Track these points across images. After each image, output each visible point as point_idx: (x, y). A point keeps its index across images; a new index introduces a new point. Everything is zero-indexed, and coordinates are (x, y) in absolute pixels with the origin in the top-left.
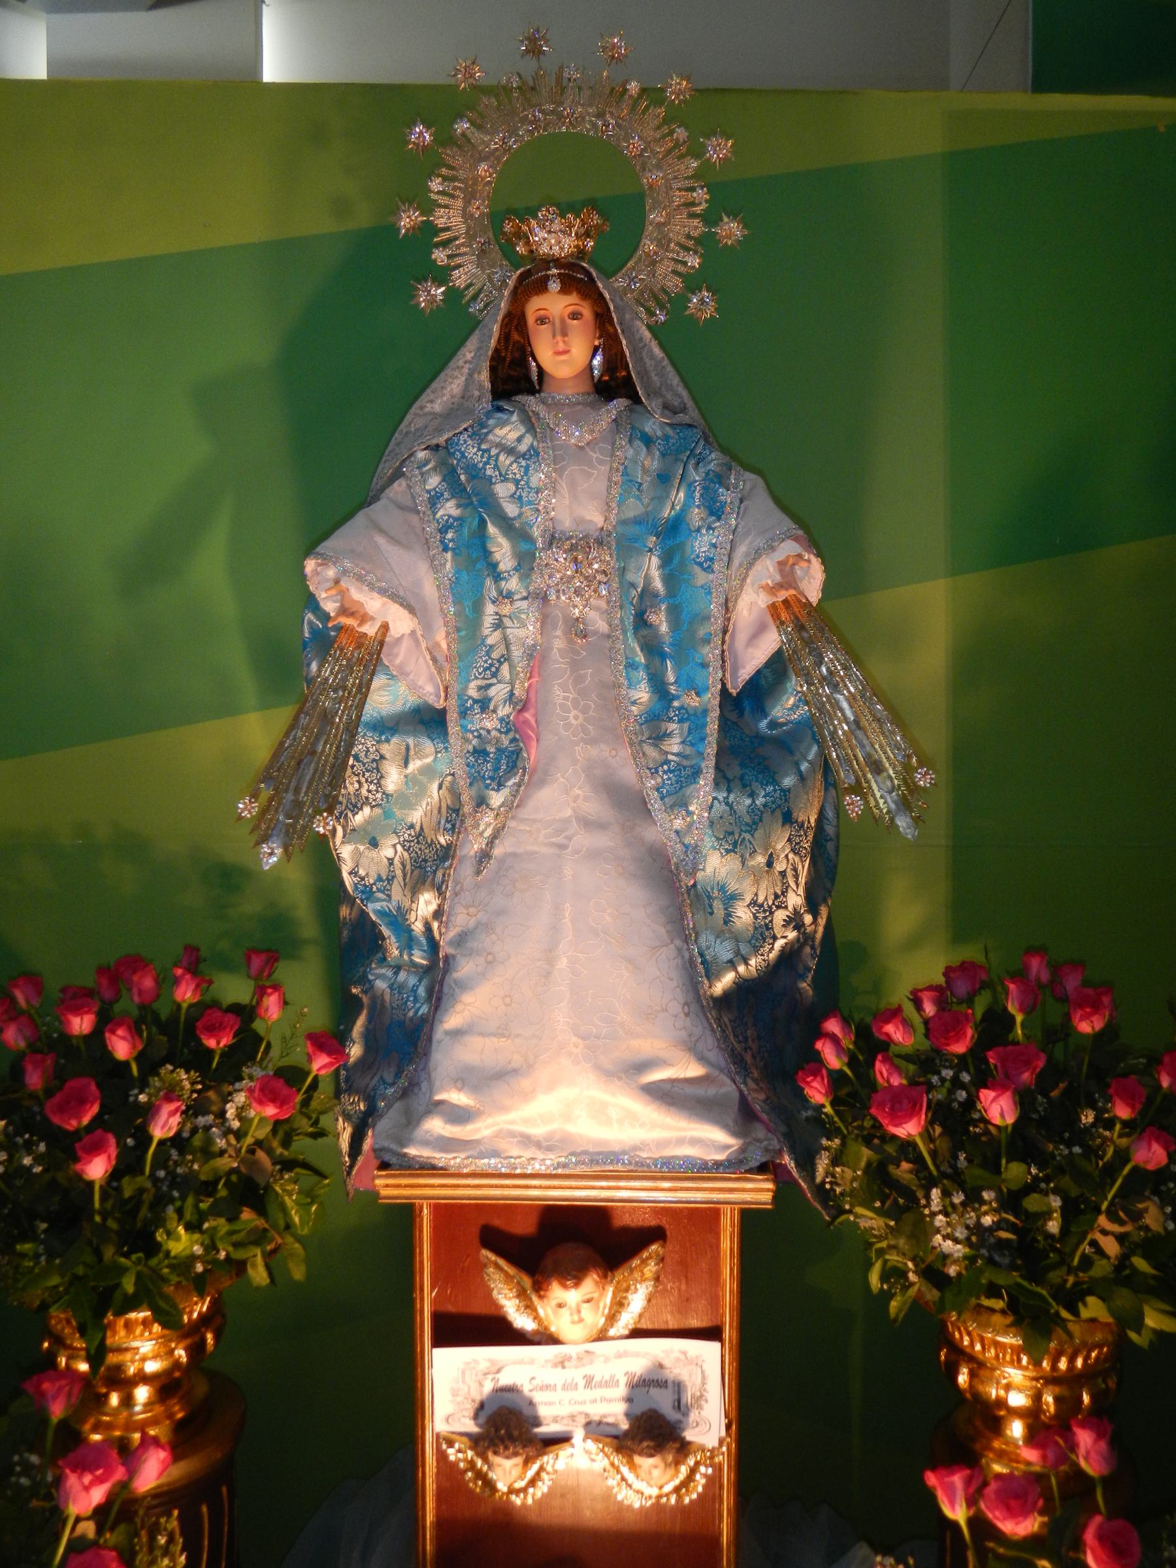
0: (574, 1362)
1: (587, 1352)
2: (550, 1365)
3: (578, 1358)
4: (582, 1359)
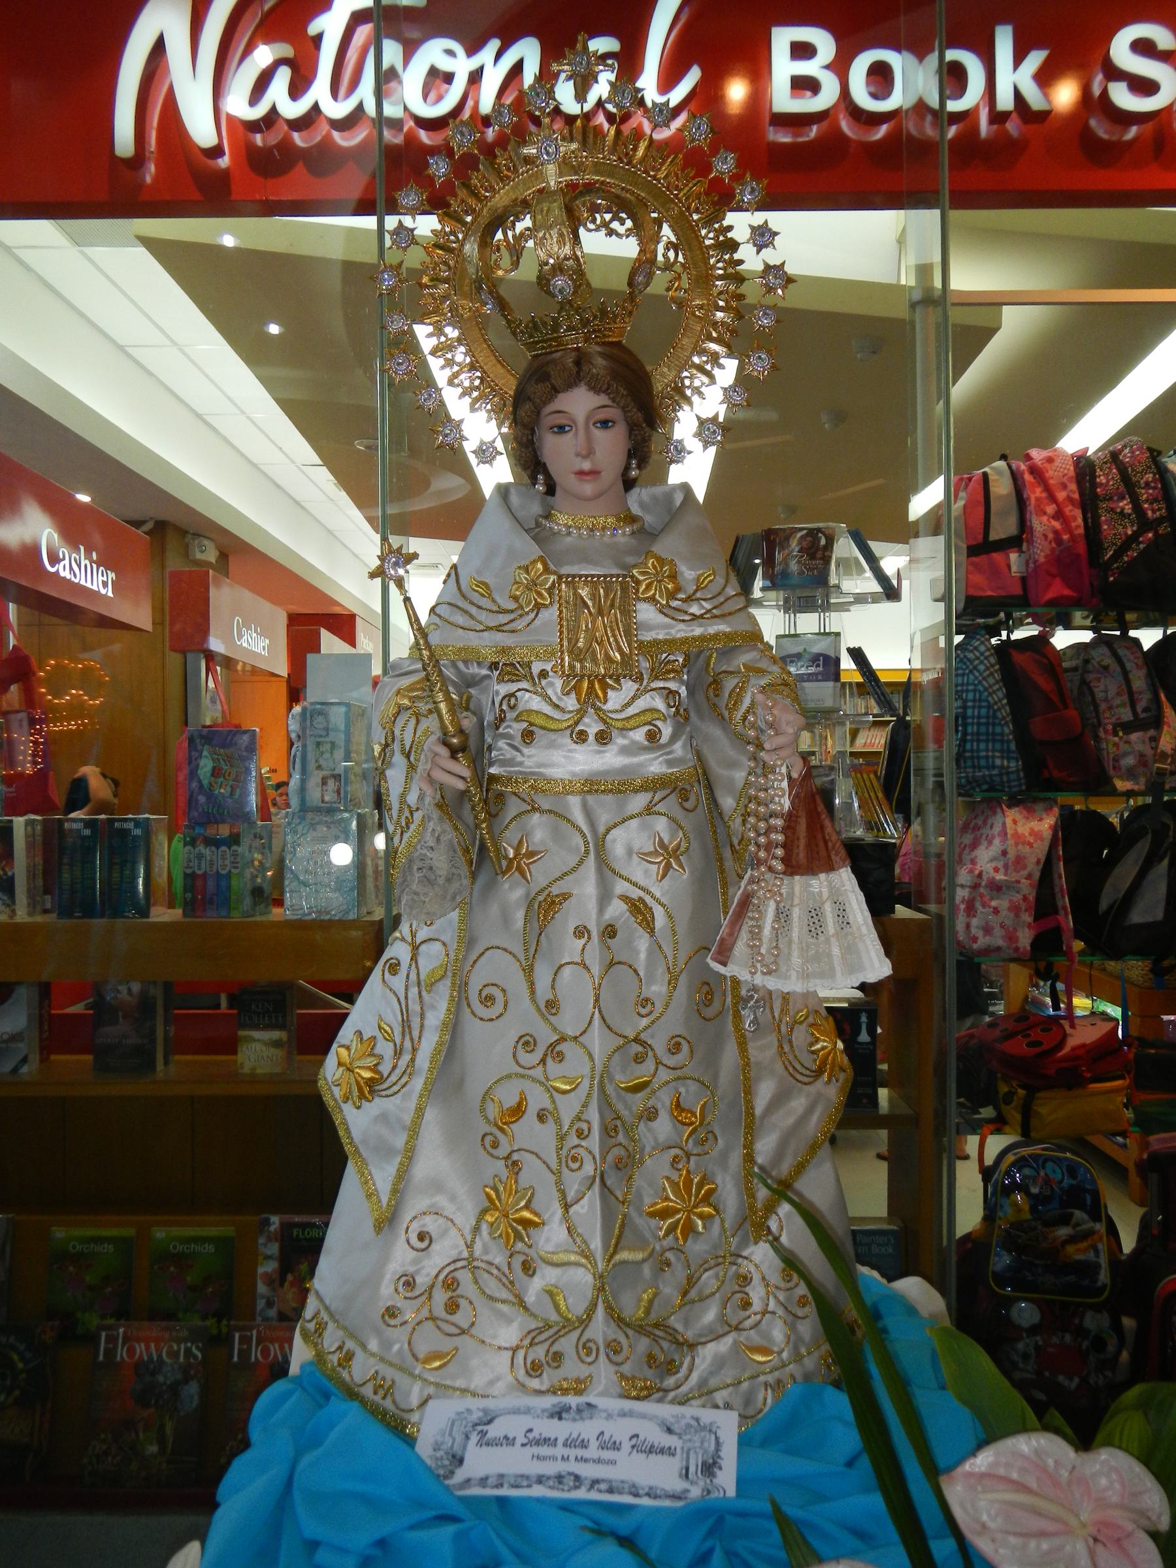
0: (573, 1413)
1: (589, 1405)
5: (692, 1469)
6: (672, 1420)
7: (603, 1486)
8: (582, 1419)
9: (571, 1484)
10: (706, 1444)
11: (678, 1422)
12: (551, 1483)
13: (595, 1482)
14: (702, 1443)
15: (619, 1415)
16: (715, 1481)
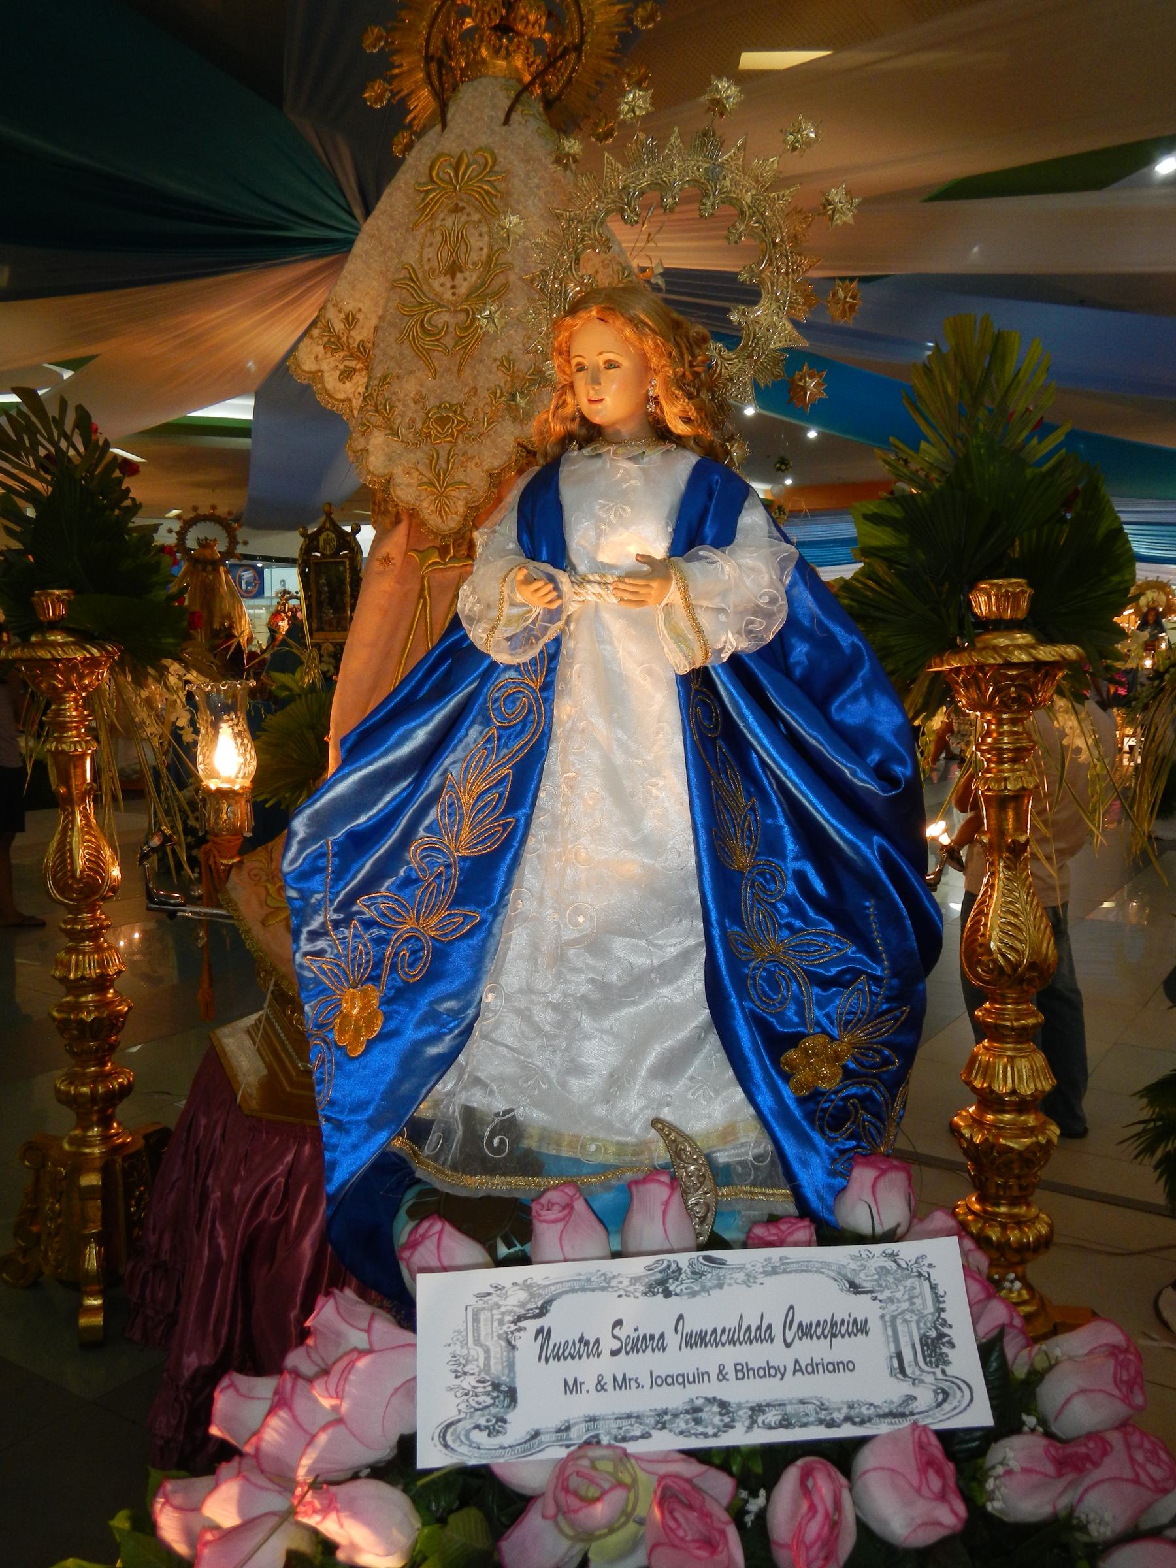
2: (642, 1289)
3: (694, 1273)
4: (702, 1274)
5: (908, 1356)
6: (853, 1265)
7: (772, 1417)
8: (704, 1289)
9: (717, 1420)
10: (918, 1301)
11: (864, 1267)
13: (757, 1410)
14: (911, 1298)
15: (766, 1273)
16: (949, 1370)
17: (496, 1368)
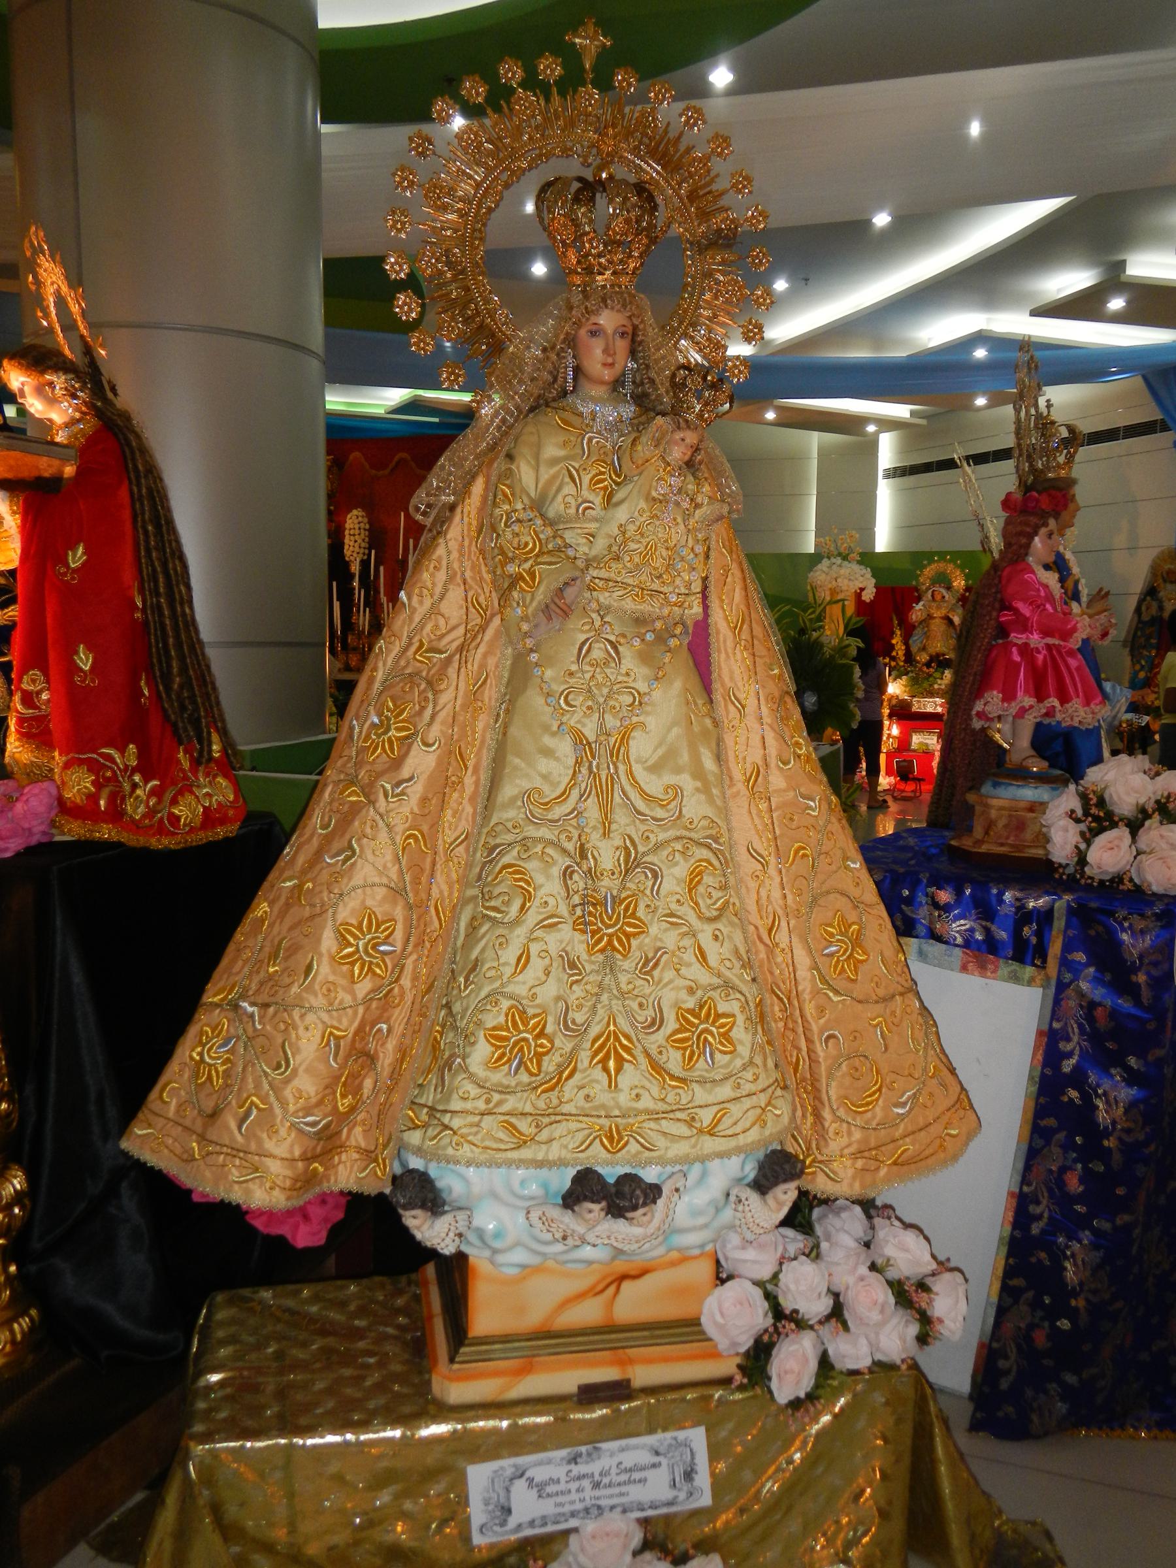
5: (677, 1479)
8: (593, 1460)
12: (581, 1515)
17: (502, 1500)
